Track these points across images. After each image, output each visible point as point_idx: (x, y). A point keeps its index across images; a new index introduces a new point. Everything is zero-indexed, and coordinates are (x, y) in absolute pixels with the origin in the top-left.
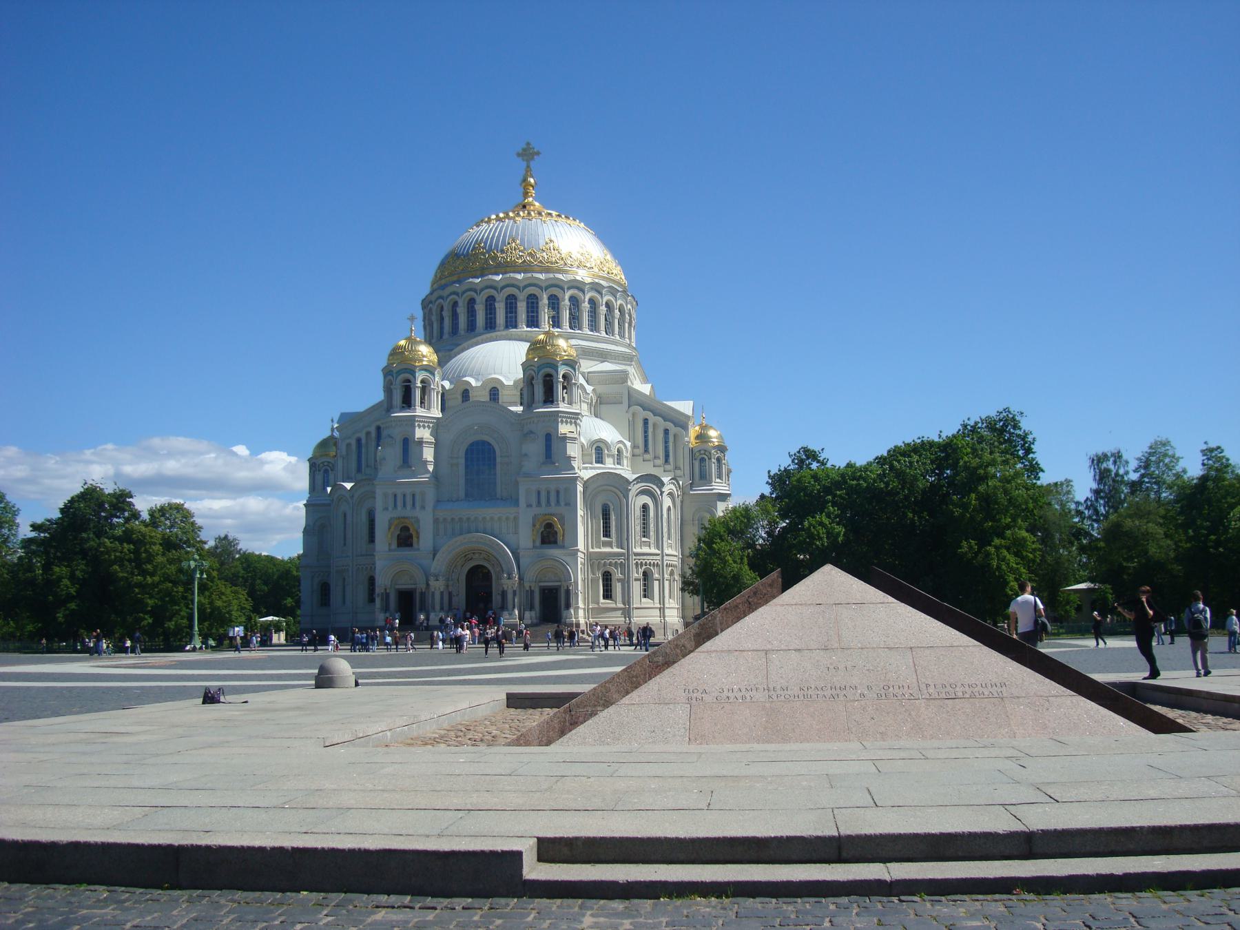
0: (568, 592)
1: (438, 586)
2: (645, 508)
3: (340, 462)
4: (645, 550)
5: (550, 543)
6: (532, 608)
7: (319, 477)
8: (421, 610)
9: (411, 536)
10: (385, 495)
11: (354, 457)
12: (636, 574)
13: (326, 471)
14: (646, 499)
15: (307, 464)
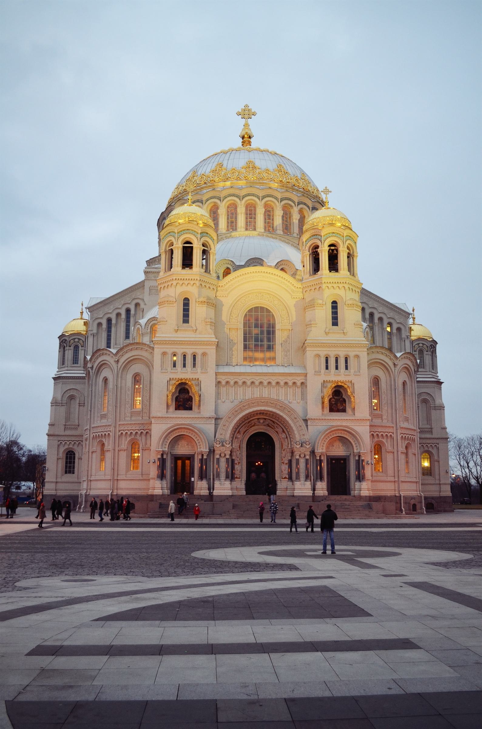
0: (359, 464)
1: (223, 451)
2: (404, 383)
3: (90, 339)
4: (405, 425)
5: (338, 411)
6: (321, 479)
7: (69, 354)
8: (201, 478)
9: (190, 399)
10: (164, 354)
11: (104, 335)
12: (402, 449)
13: (76, 348)
14: (404, 377)
15: (58, 341)
